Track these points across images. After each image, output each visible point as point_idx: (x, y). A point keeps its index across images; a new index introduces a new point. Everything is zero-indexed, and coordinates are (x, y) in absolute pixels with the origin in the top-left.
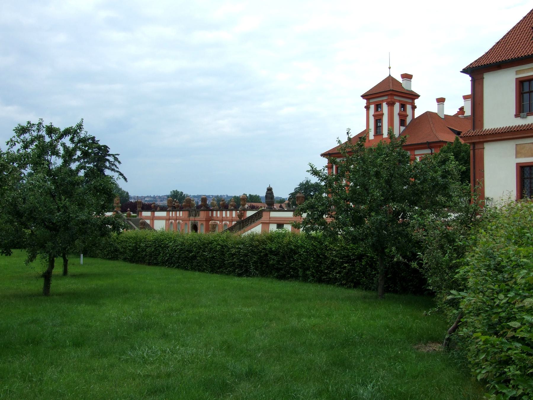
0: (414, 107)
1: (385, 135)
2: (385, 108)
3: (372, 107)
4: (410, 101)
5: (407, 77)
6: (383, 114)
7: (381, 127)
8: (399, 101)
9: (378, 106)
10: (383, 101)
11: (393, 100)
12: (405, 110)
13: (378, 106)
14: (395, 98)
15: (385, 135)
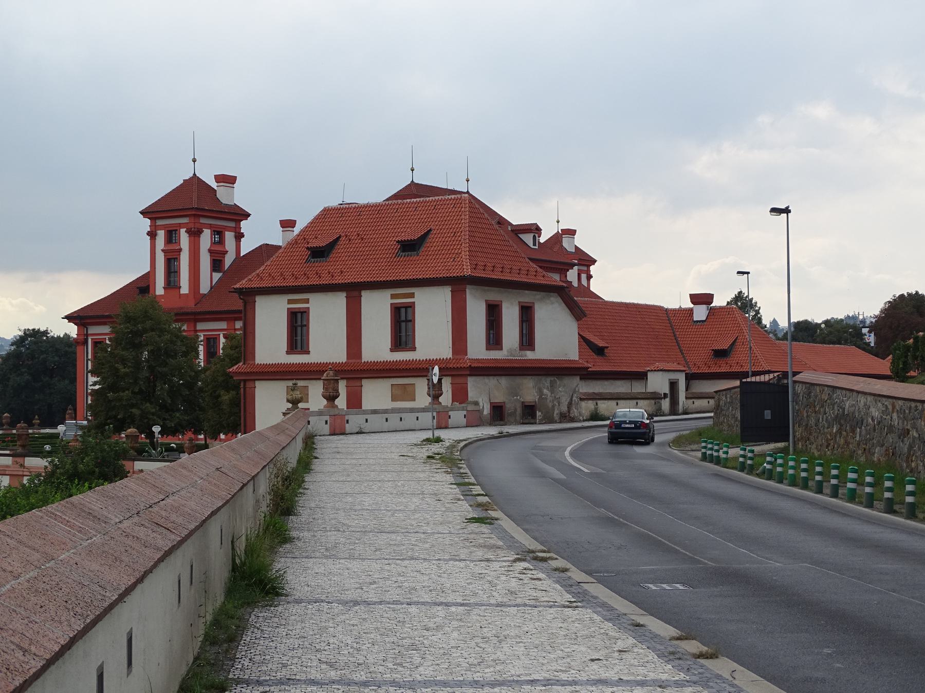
0: (239, 236)
1: (185, 289)
2: (184, 240)
3: (161, 234)
4: (232, 224)
5: (228, 180)
6: (180, 250)
7: (177, 272)
8: (210, 226)
9: (172, 236)
10: (181, 226)
11: (198, 225)
12: (221, 242)
13: (172, 236)
14: (203, 221)
15: (185, 289)
